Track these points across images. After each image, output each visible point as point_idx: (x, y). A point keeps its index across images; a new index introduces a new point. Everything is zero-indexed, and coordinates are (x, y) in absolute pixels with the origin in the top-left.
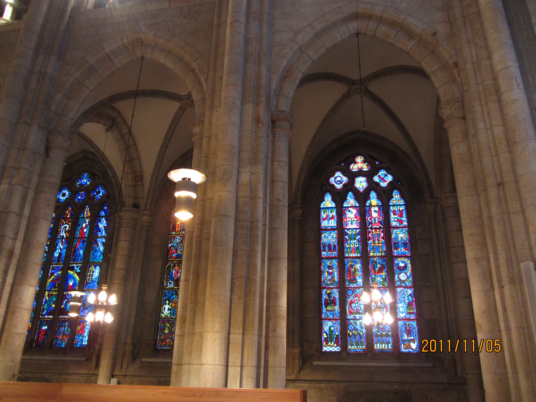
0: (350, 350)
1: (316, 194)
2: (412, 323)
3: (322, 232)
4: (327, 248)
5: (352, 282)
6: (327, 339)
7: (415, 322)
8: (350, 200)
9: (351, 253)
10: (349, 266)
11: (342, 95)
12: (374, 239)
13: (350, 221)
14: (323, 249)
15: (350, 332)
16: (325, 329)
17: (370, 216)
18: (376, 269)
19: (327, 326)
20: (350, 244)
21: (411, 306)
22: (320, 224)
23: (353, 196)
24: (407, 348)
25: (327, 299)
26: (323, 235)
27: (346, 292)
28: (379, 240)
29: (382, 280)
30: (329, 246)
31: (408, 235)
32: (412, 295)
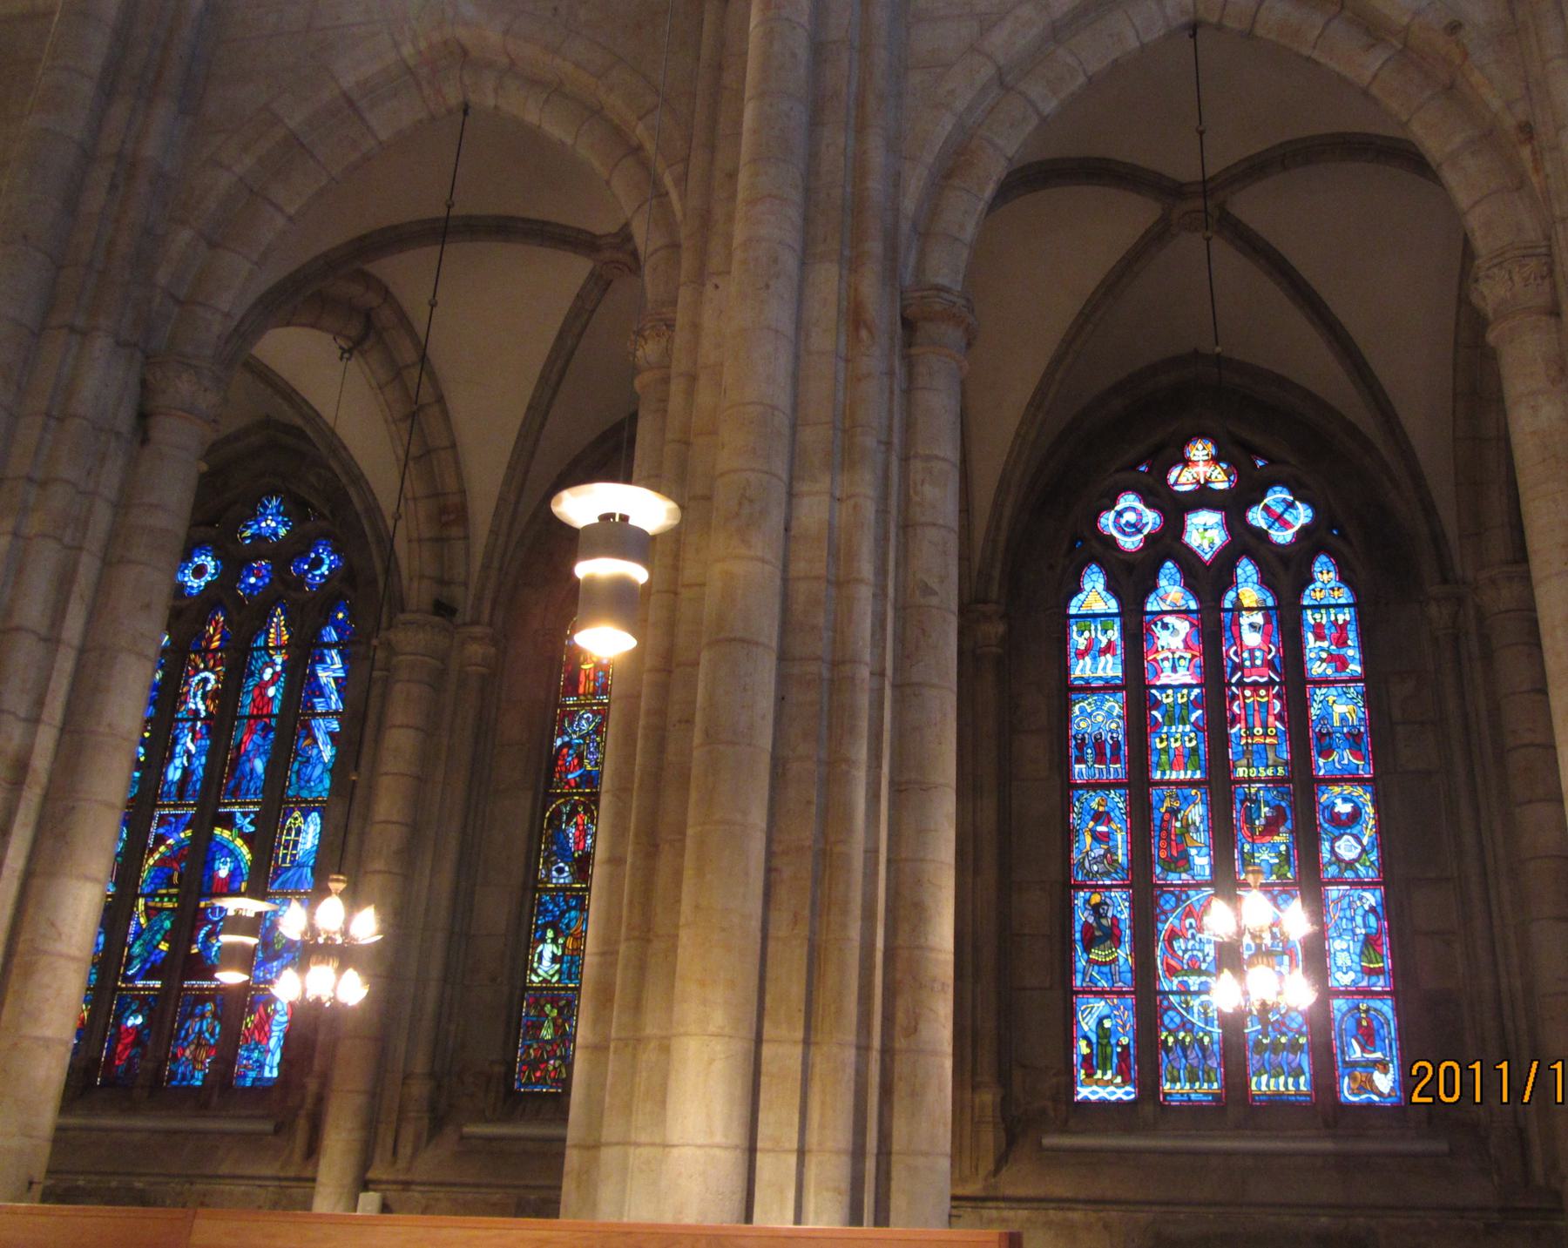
0: (1168, 1098)
1: (1051, 567)
2: (1377, 1004)
3: (1073, 696)
4: (1089, 751)
5: (1176, 868)
6: (1092, 1059)
7: (1389, 1002)
8: (1169, 589)
9: (1172, 769)
10: (1166, 811)
11: (1140, 234)
12: (1250, 719)
13: (1167, 659)
14: (1077, 754)
15: (1170, 1034)
16: (1083, 1024)
17: (1235, 644)
18: (1257, 822)
19: (1091, 1015)
20: (1167, 739)
21: (1374, 950)
22: (1066, 670)
23: (1178, 576)
24: (1361, 1089)
25: (1091, 925)
26: (1077, 706)
27: (1155, 902)
28: (1265, 726)
29: (1277, 861)
30: (1099, 745)
31: (1364, 707)
32: (1379, 909)
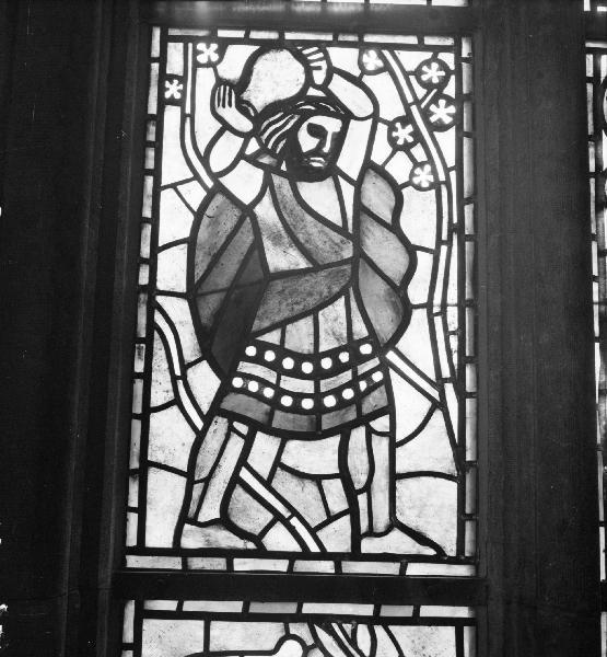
25: (247, 211)
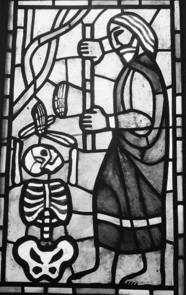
32: (164, 61)
